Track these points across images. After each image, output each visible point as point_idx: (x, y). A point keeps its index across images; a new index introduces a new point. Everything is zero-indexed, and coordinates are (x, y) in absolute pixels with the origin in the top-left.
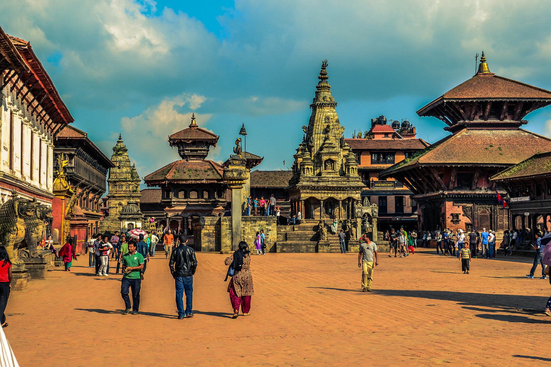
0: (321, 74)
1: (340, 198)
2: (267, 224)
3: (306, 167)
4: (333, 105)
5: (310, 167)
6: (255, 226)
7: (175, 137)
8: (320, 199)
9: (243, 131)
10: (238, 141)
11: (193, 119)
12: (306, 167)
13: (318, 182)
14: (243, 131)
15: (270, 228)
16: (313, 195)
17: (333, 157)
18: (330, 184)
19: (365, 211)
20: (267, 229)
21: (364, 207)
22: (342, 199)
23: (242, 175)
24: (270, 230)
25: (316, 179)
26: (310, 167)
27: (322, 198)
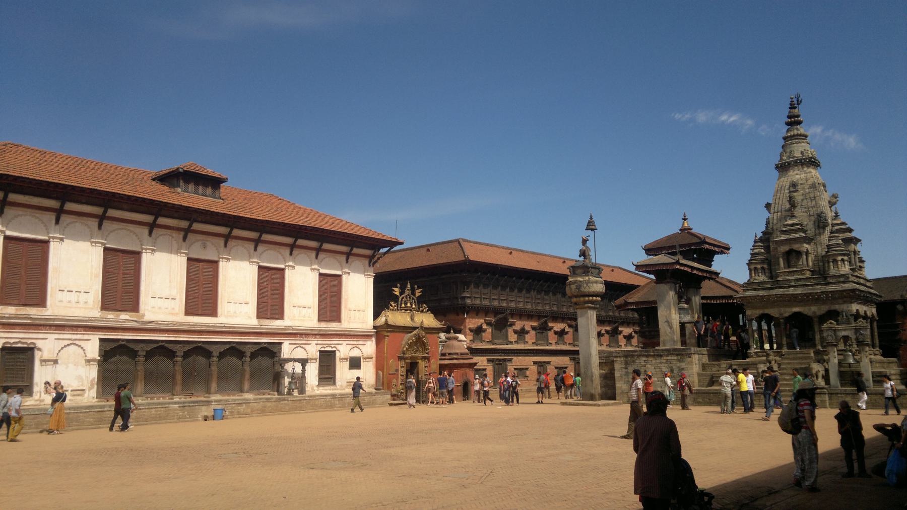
0: (789, 117)
1: (814, 312)
2: (679, 361)
3: (752, 267)
4: (813, 163)
5: (759, 266)
6: (661, 363)
7: (651, 247)
8: (777, 316)
9: (591, 226)
10: (584, 242)
11: (685, 219)
12: (752, 267)
13: (771, 288)
14: (591, 226)
15: (683, 365)
16: (767, 311)
17: (796, 247)
18: (791, 291)
19: (844, 333)
20: (679, 367)
21: (840, 327)
22: (819, 313)
23: (582, 289)
24: (683, 369)
25: (768, 286)
26: (759, 266)
27: (781, 314)
